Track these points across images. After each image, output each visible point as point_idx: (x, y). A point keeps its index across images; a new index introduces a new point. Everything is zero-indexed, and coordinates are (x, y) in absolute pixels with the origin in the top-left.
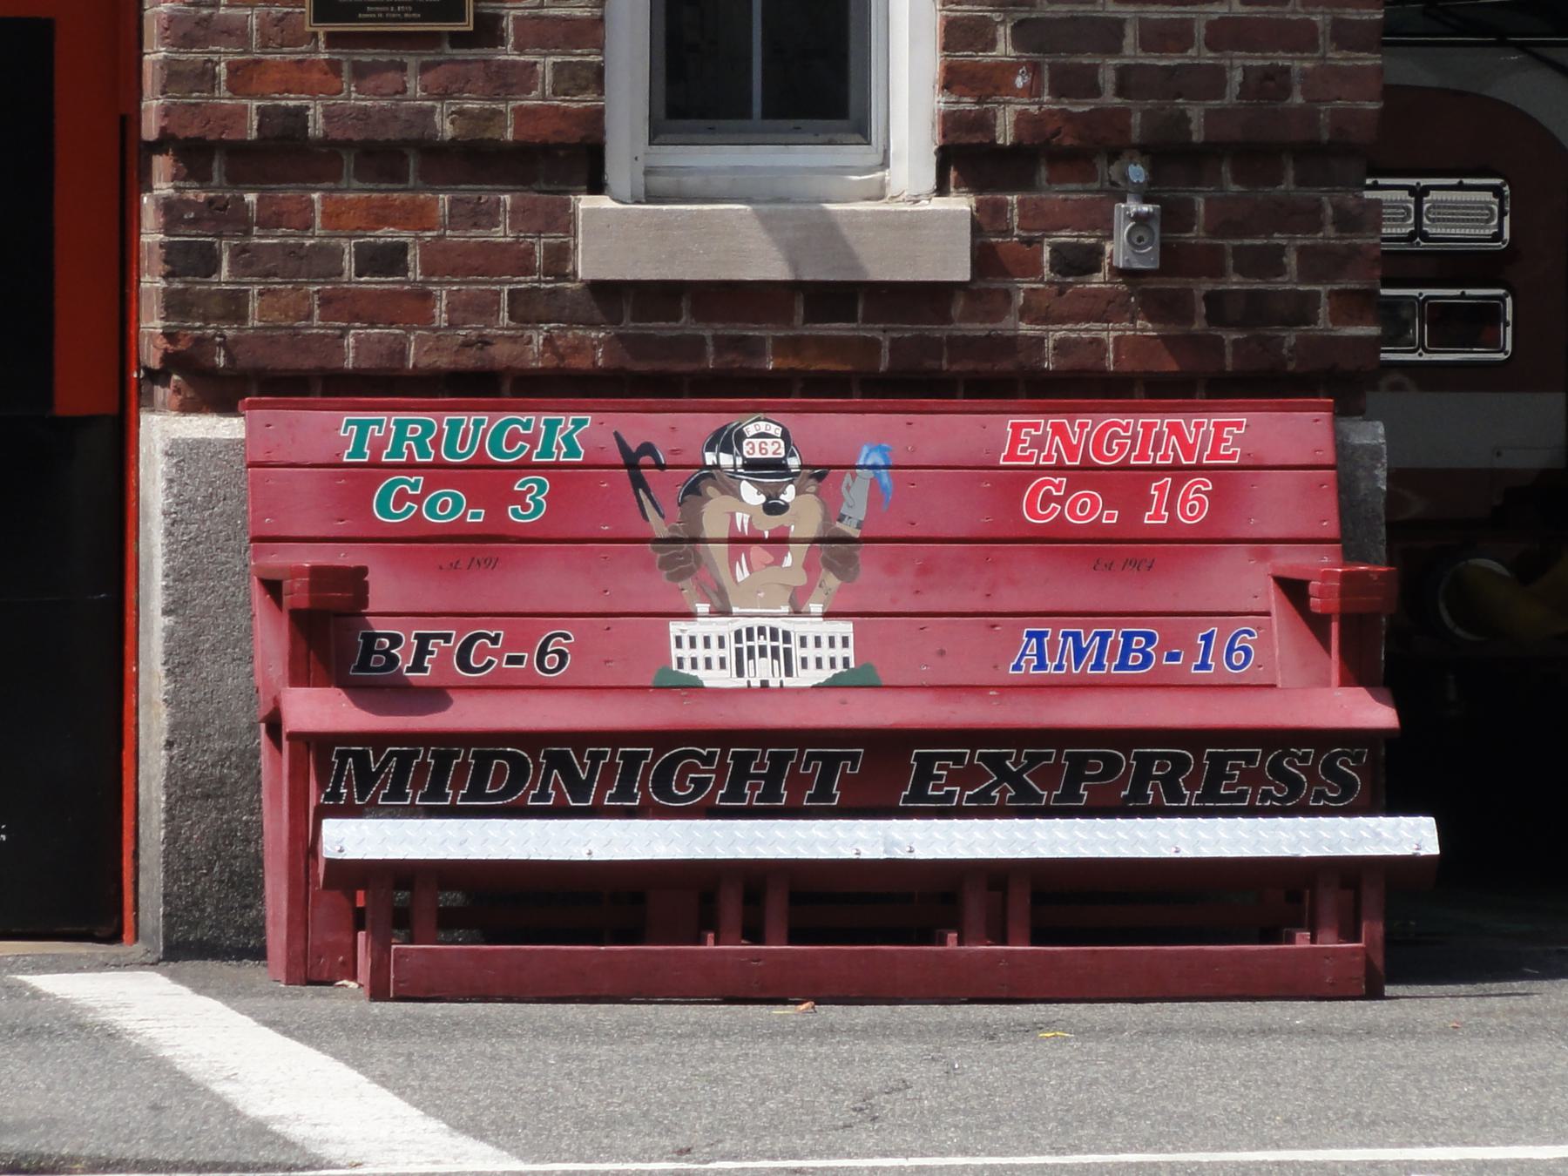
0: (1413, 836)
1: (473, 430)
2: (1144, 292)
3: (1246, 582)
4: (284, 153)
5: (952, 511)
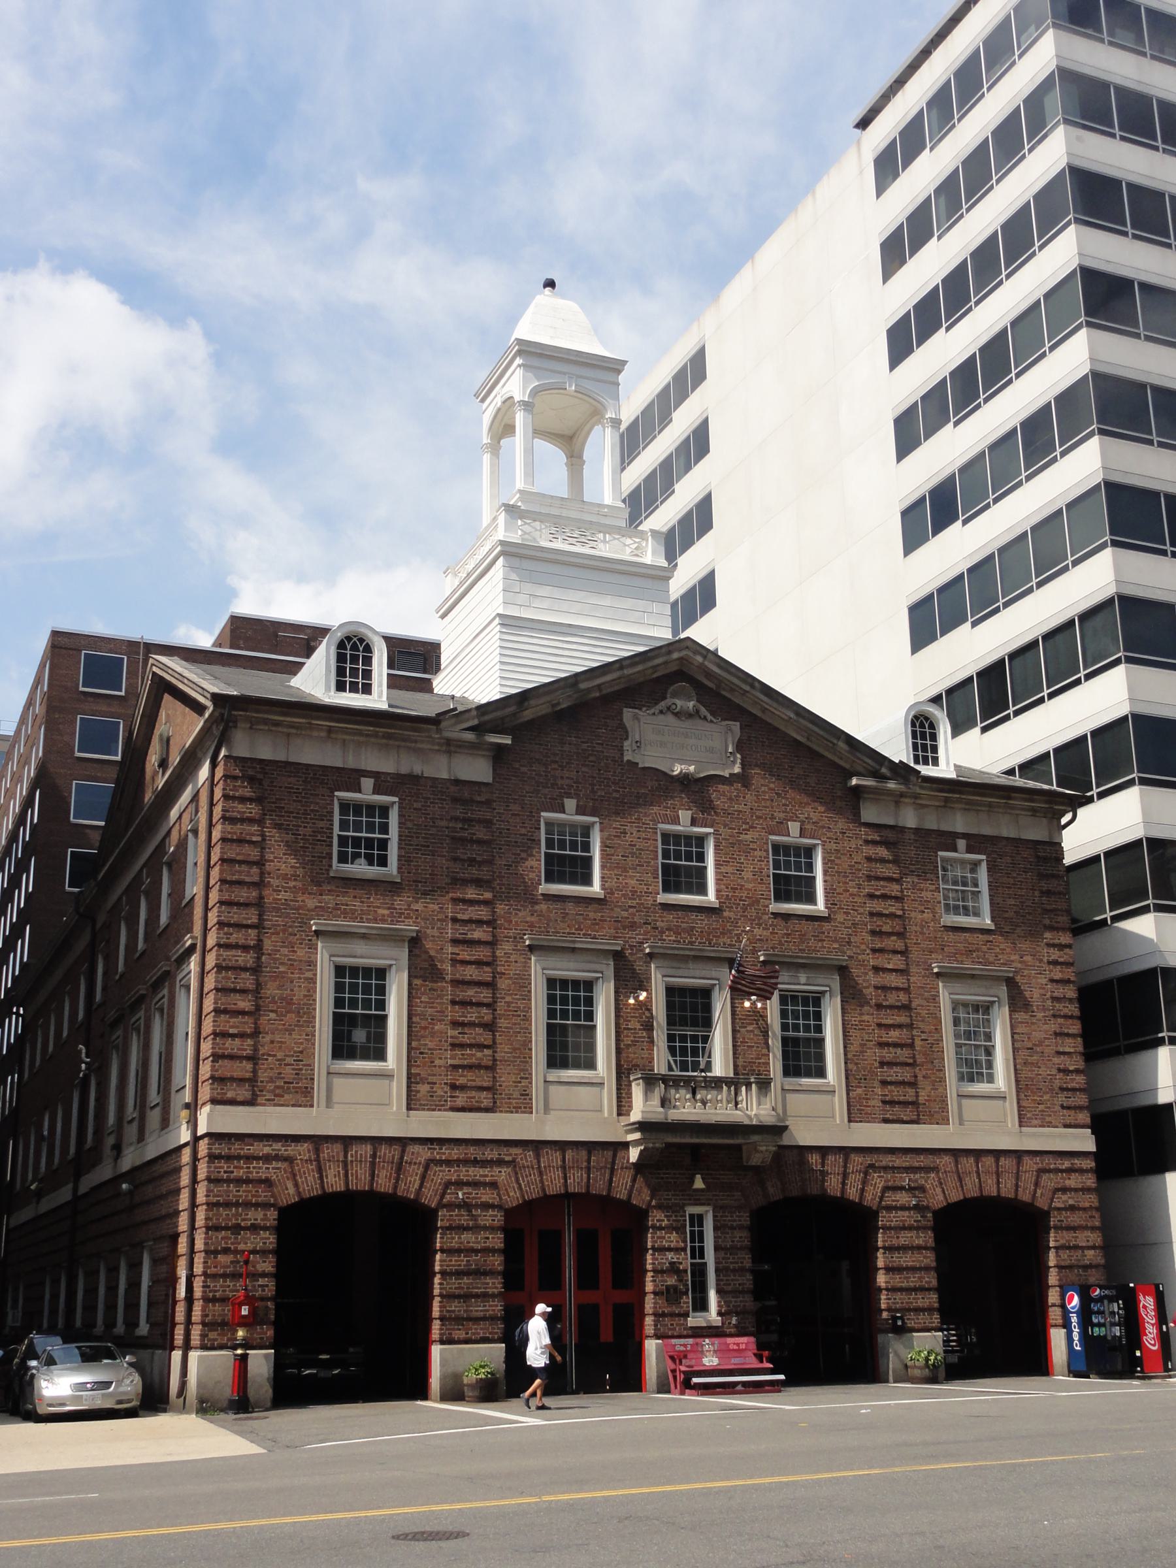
0: (782, 1377)
1: (682, 1341)
2: (736, 1326)
3: (750, 1354)
4: (663, 1315)
5: (723, 1347)
